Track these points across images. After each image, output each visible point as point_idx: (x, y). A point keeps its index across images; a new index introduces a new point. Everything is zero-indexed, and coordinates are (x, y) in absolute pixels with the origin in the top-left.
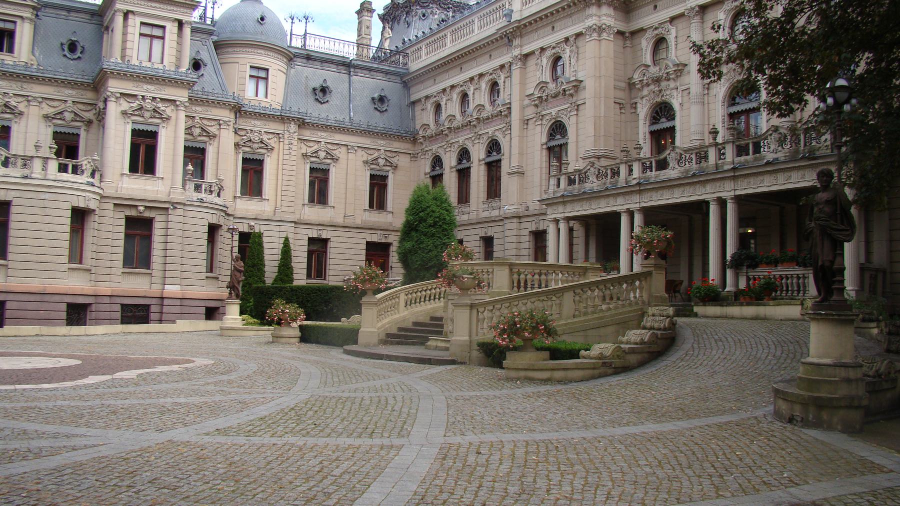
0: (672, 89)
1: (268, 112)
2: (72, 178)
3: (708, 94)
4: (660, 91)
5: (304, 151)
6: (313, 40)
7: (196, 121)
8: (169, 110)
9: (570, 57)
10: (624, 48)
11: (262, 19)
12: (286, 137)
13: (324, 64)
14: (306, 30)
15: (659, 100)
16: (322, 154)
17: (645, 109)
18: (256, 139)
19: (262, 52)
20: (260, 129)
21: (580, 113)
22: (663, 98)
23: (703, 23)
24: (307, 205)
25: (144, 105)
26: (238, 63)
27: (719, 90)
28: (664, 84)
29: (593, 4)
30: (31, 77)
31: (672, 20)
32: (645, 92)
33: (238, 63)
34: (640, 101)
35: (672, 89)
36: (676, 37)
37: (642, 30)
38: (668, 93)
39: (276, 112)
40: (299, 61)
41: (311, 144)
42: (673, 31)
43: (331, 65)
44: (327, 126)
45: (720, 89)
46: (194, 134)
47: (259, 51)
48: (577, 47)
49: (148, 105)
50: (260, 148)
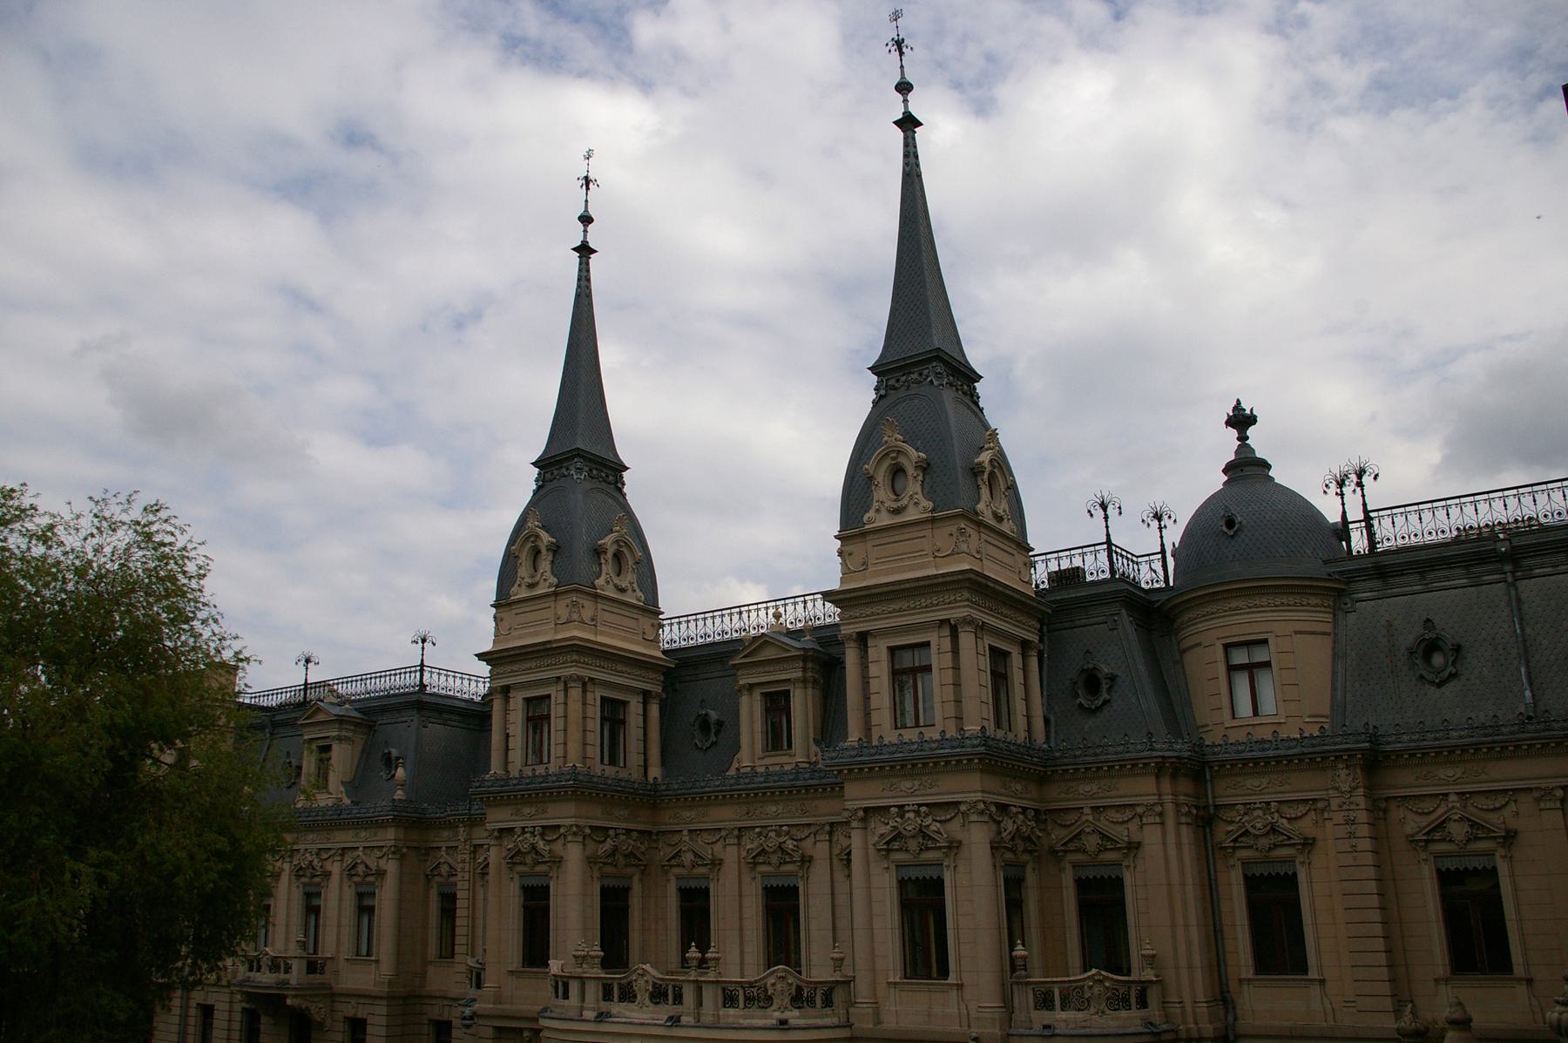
1: (1271, 753)
2: (745, 1017)
5: (1409, 831)
6: (1387, 522)
7: (1084, 818)
8: (955, 828)
11: (1230, 523)
12: (1334, 804)
13: (1430, 576)
14: (1364, 505)
16: (1458, 830)
18: (1259, 826)
19: (1241, 603)
20: (1267, 798)
24: (1447, 980)
25: (901, 829)
26: (1199, 645)
30: (807, 788)
33: (1199, 645)
39: (1290, 748)
40: (1364, 591)
41: (1427, 805)
43: (1445, 573)
44: (1452, 749)
46: (1088, 848)
47: (1234, 604)
49: (911, 823)
50: (1276, 846)
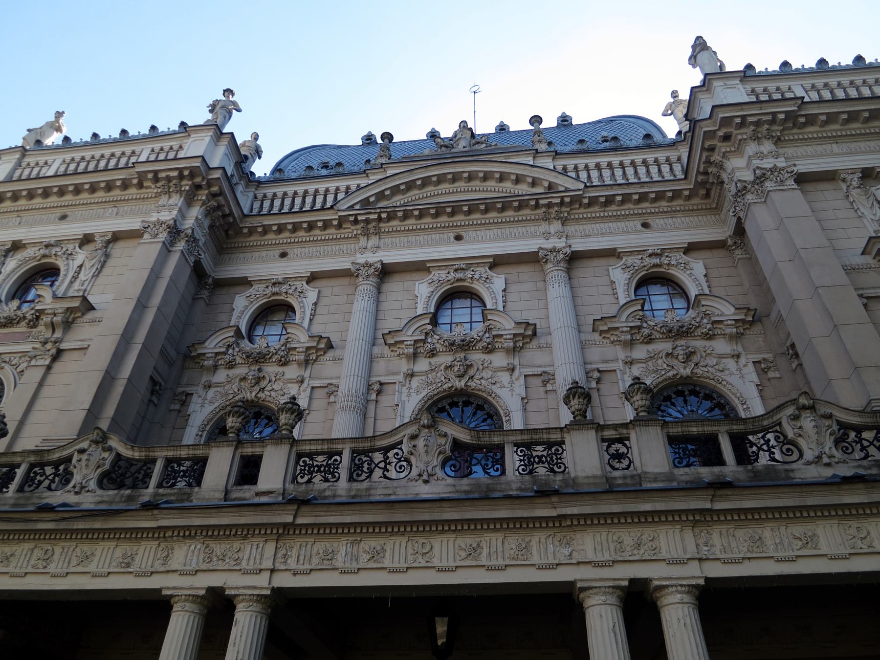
0: (290, 381)
3: (377, 401)
4: (259, 380)
9: (80, 267)
10: (194, 299)
15: (250, 396)
17: (209, 409)
21: (57, 366)
22: (261, 395)
23: (379, 293)
27: (404, 397)
28: (271, 369)
29: (180, 192)
31: (313, 278)
32: (221, 376)
34: (200, 390)
35: (290, 381)
36: (315, 304)
37: (245, 282)
38: (276, 386)
42: (312, 295)
45: (409, 396)
48: (107, 256)
